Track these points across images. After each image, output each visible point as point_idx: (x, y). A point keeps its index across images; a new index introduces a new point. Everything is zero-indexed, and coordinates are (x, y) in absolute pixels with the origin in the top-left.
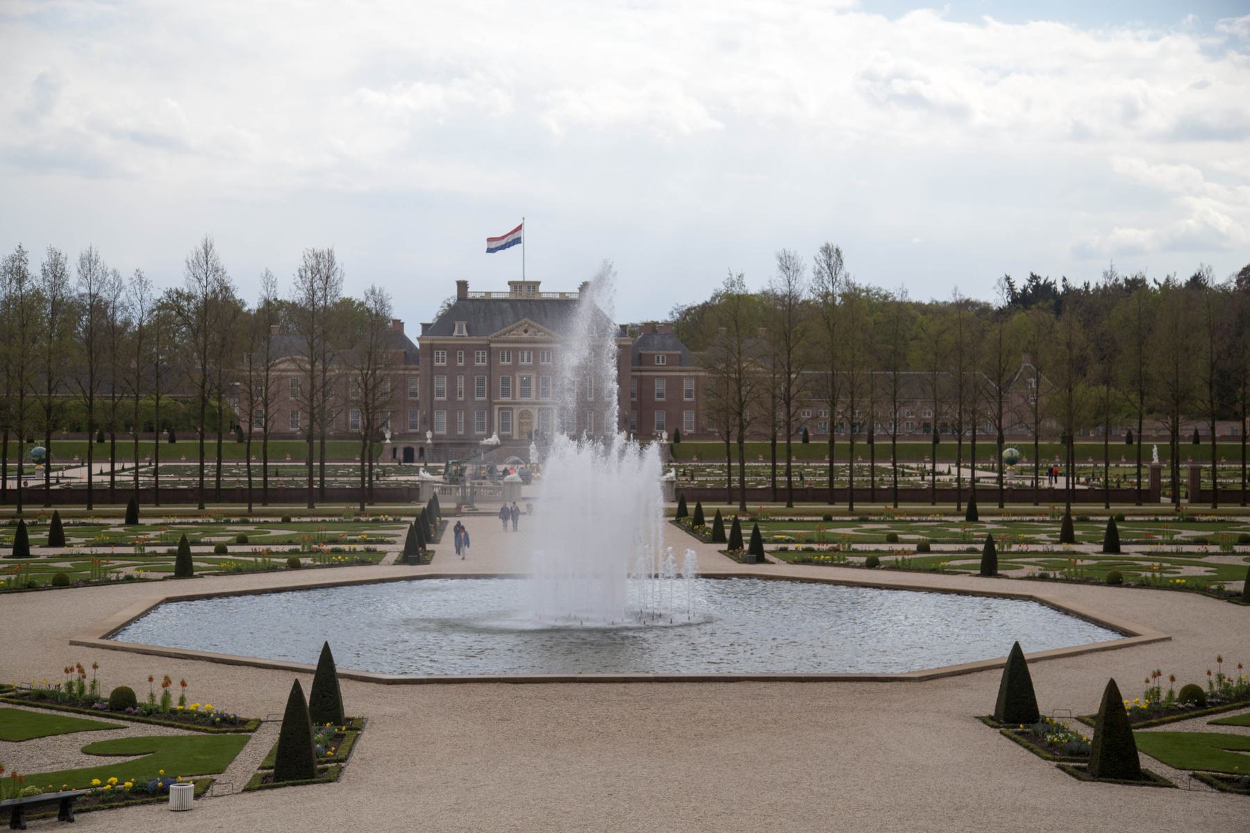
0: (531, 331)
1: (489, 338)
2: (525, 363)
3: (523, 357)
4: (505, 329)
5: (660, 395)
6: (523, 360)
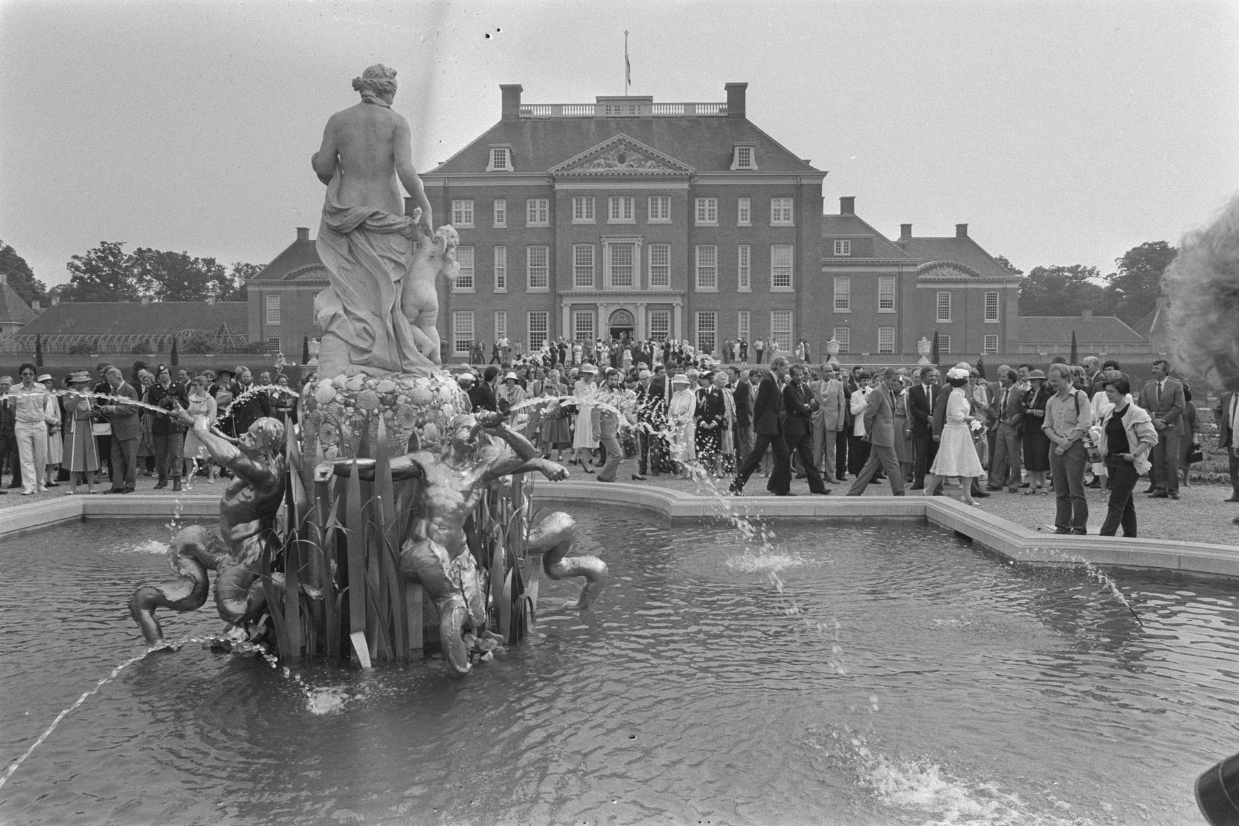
0: (632, 157)
1: (552, 170)
2: (622, 219)
3: (616, 208)
4: (581, 155)
5: (843, 303)
6: (616, 215)
